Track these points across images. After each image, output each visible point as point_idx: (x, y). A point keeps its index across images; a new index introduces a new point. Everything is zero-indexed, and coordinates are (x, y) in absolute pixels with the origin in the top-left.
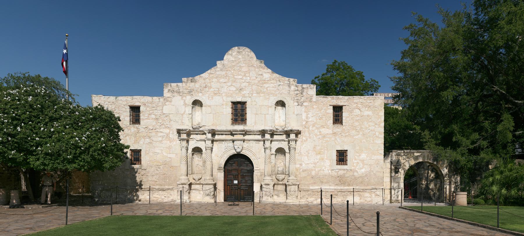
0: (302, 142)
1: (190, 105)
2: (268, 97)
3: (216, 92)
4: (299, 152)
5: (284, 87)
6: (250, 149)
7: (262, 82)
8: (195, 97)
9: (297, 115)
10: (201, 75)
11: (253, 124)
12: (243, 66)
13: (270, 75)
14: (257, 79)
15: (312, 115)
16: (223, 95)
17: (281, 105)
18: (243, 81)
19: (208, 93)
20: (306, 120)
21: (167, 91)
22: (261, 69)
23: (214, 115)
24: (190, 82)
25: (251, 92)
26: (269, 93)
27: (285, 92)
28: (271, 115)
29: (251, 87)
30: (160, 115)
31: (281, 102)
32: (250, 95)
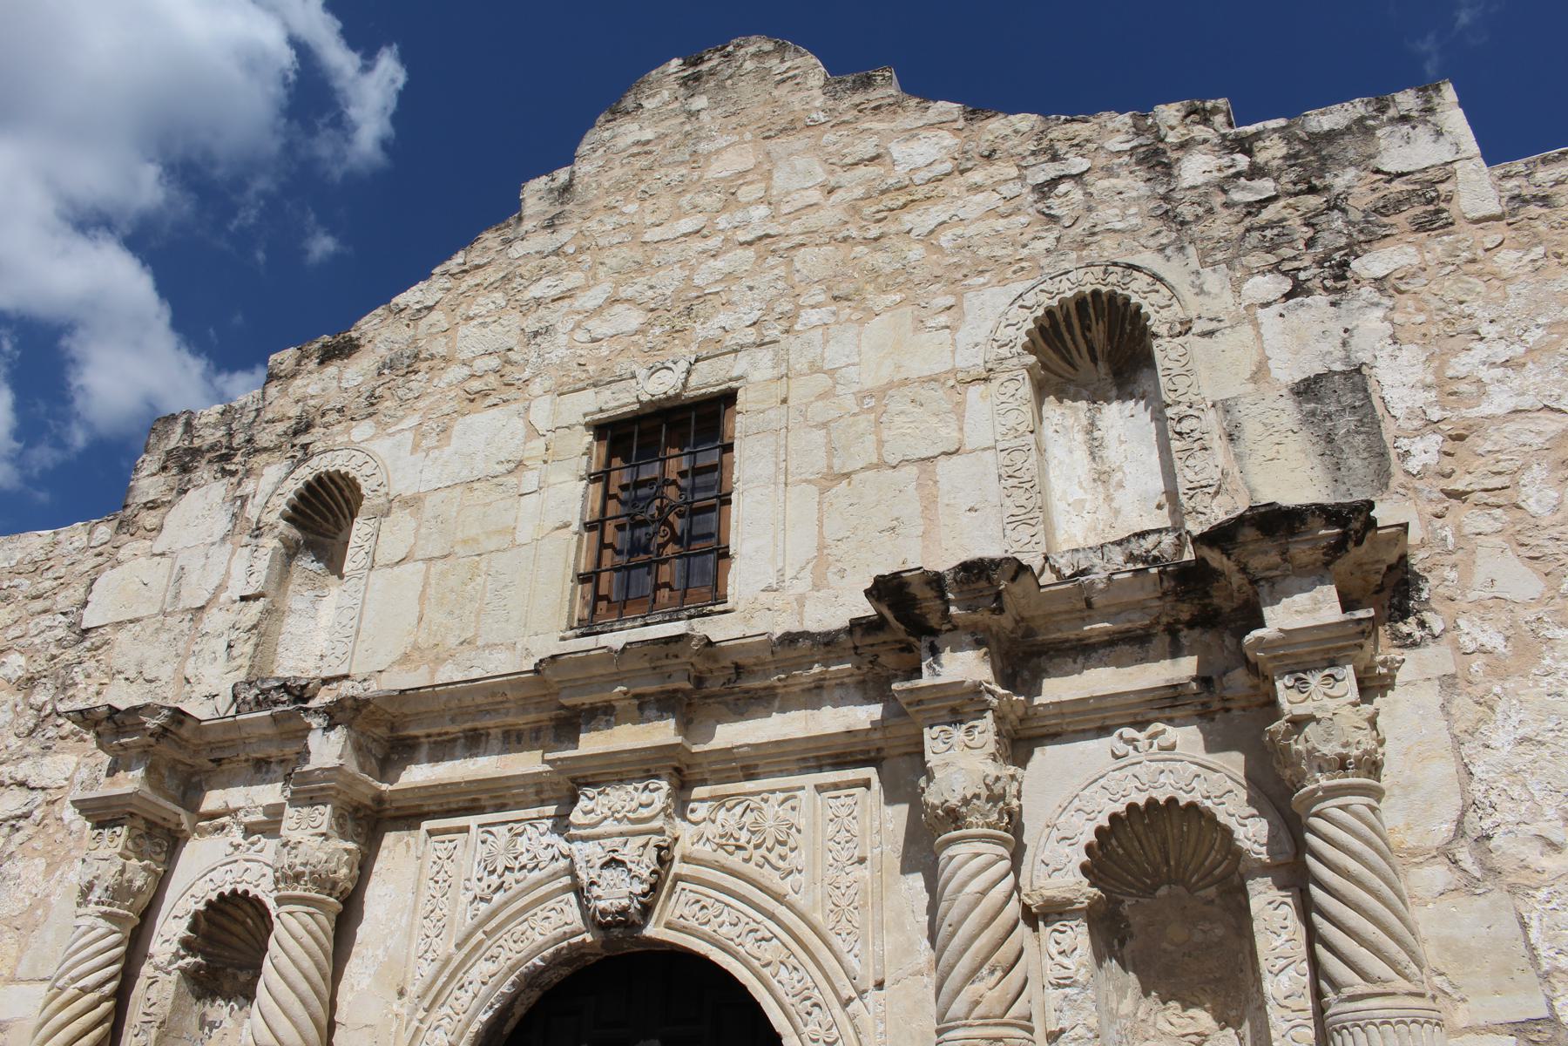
0: (1449, 683)
1: (273, 527)
2: (950, 300)
3: (476, 385)
4: (1445, 829)
5: (1106, 183)
6: (750, 869)
7: (887, 201)
8: (314, 462)
9: (1307, 390)
10: (400, 300)
11: (803, 586)
12: (718, 152)
13: (948, 140)
14: (833, 198)
15: (1502, 352)
16: (536, 388)
17: (1103, 368)
18: (714, 242)
19: (421, 404)
20: (1435, 414)
21: (155, 467)
22: (867, 125)
23: (439, 566)
24: (312, 364)
25: (785, 306)
26: (958, 266)
27: (1124, 218)
28: (989, 455)
29: (776, 271)
30: (59, 642)
31: (1099, 332)
32: (773, 332)
